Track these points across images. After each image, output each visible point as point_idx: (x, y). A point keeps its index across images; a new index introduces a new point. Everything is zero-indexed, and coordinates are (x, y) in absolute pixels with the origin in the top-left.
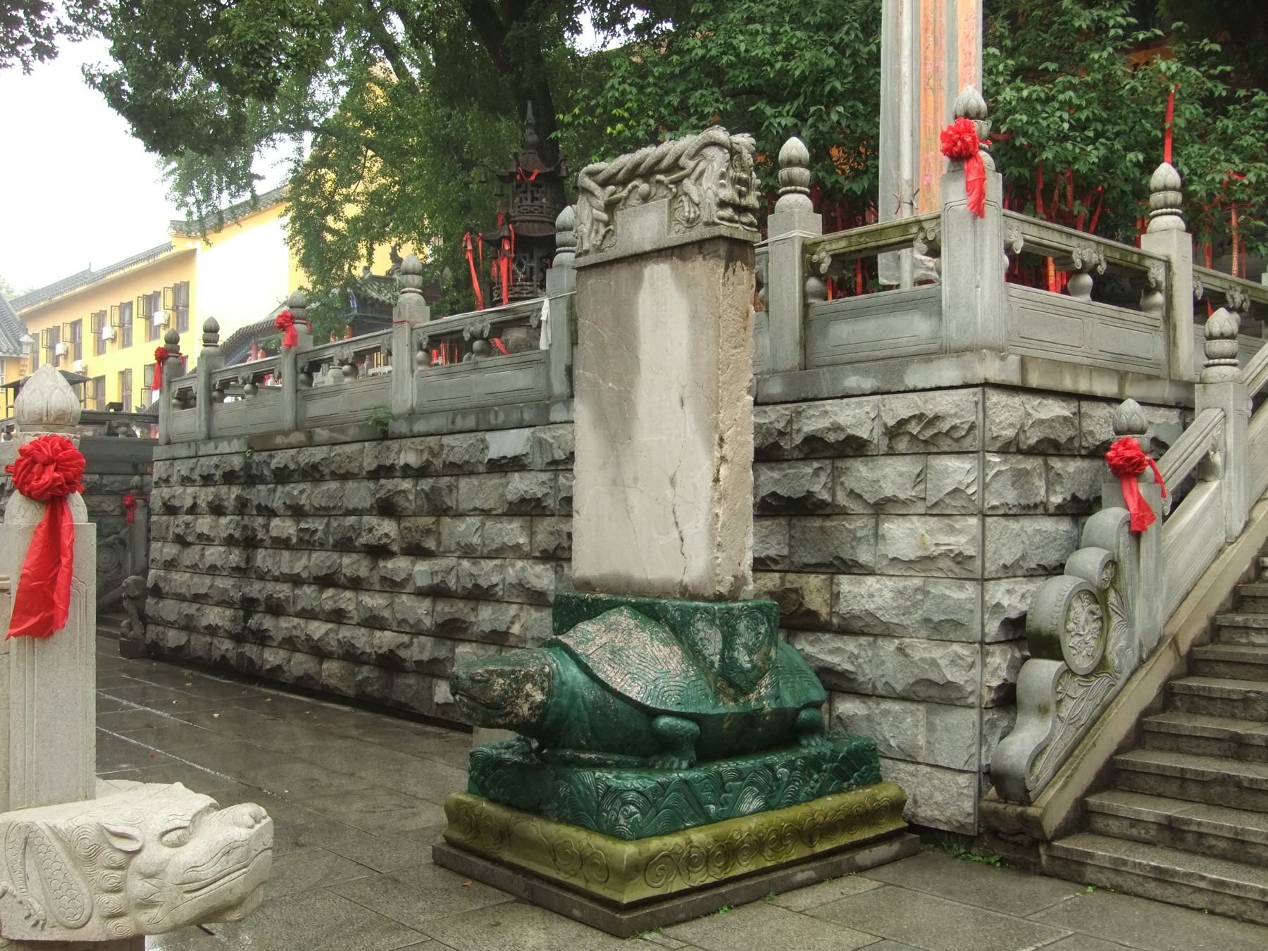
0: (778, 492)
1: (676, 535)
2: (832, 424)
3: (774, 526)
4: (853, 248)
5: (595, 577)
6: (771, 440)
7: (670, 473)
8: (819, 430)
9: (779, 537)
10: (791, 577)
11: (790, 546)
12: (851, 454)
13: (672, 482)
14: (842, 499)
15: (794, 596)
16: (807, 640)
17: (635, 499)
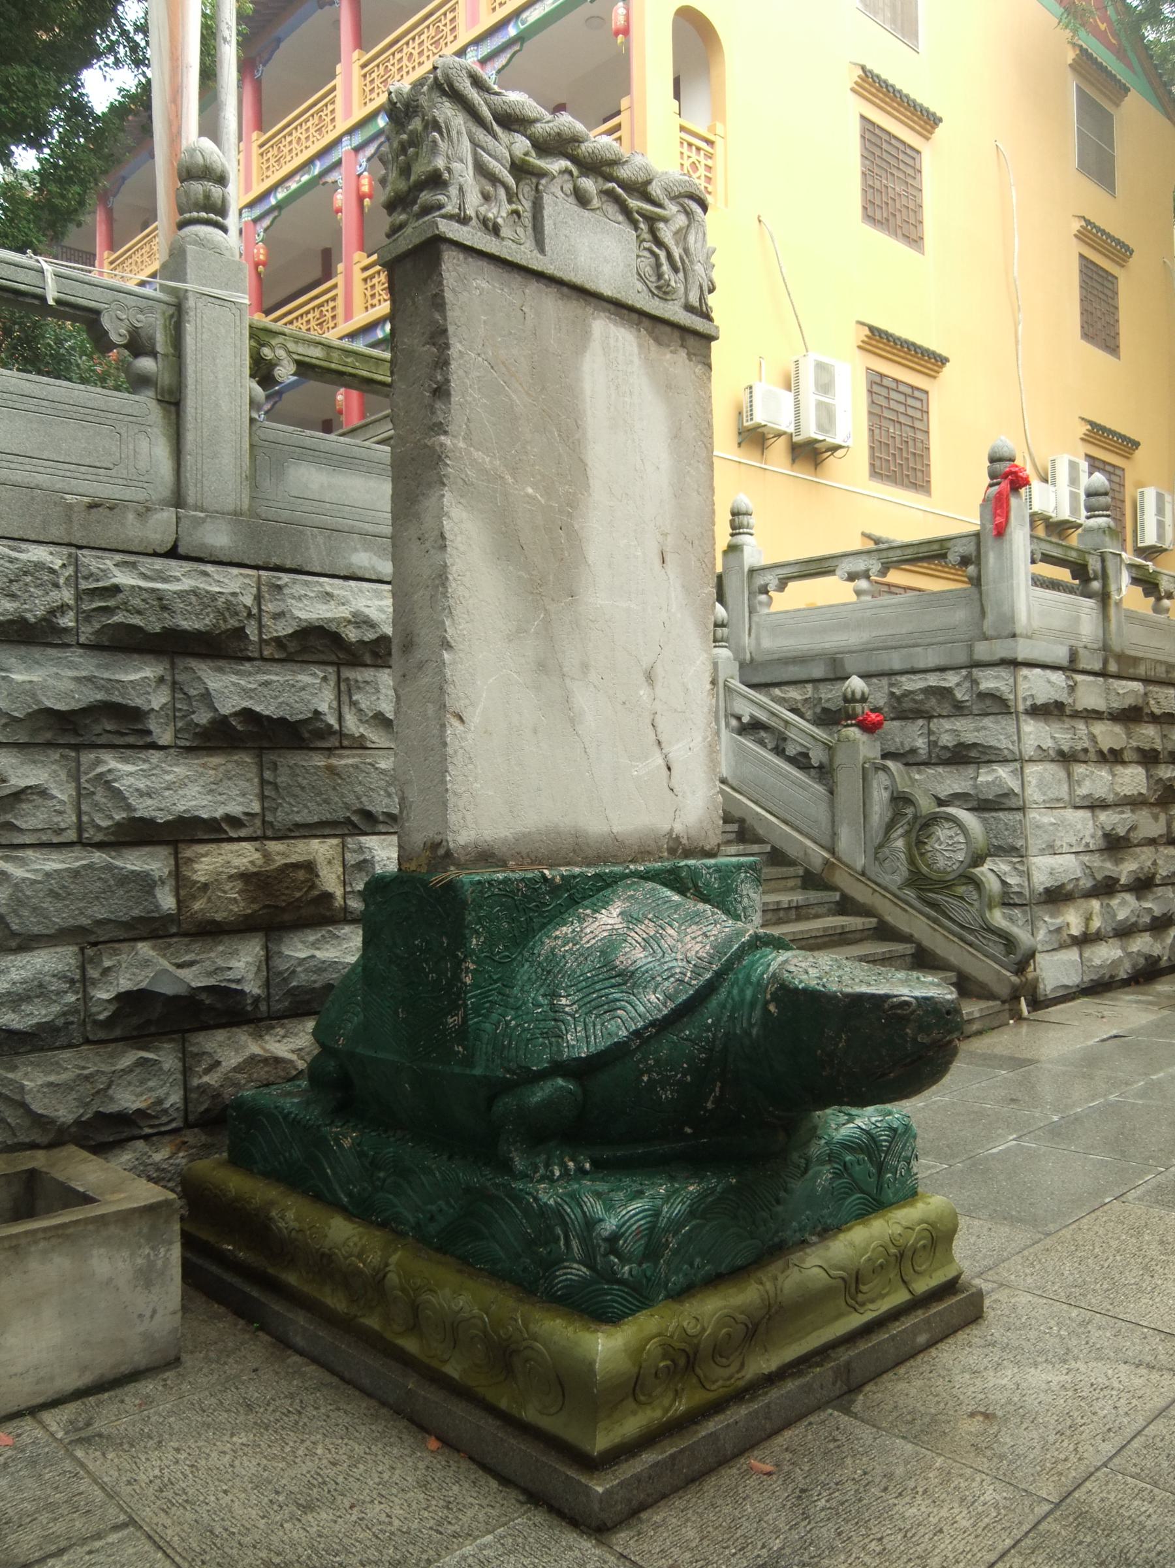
0: (258, 709)
1: (660, 761)
2: (354, 615)
3: (230, 766)
4: (333, 366)
5: (506, 839)
6: (233, 623)
7: (646, 662)
8: (331, 620)
9: (243, 784)
10: (274, 846)
11: (263, 798)
12: (369, 662)
13: (649, 677)
14: (352, 724)
15: (301, 875)
16: (303, 942)
17: (583, 698)
